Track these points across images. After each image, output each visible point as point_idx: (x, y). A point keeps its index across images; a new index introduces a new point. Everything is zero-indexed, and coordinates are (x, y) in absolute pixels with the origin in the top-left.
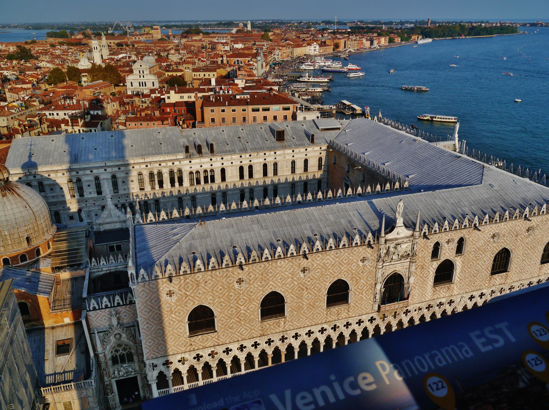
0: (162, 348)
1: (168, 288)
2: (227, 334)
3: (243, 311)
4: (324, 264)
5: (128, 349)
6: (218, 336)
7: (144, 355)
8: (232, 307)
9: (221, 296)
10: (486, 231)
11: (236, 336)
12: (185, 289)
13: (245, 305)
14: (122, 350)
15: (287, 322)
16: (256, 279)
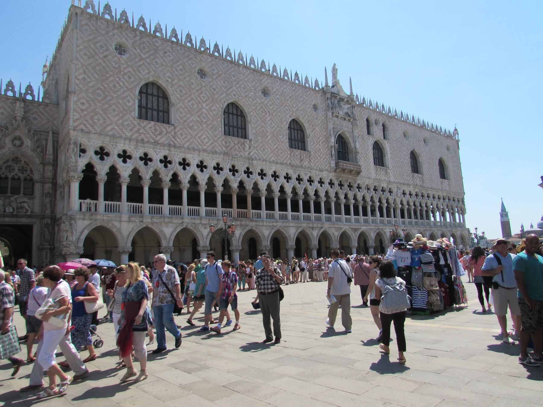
0: (98, 120)
1: (120, 37)
2: (186, 134)
3: (204, 110)
4: (282, 91)
5: (29, 172)
6: (175, 133)
7: (71, 121)
8: (192, 99)
9: (182, 78)
10: (399, 125)
11: (196, 143)
12: (140, 48)
13: (207, 102)
14: (19, 170)
15: (252, 148)
16: (220, 75)
